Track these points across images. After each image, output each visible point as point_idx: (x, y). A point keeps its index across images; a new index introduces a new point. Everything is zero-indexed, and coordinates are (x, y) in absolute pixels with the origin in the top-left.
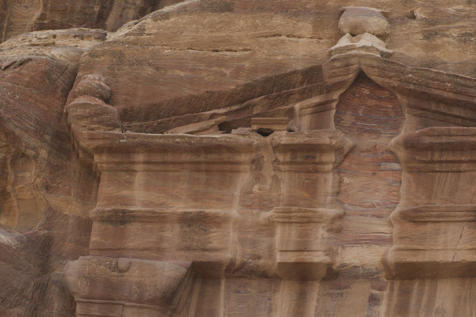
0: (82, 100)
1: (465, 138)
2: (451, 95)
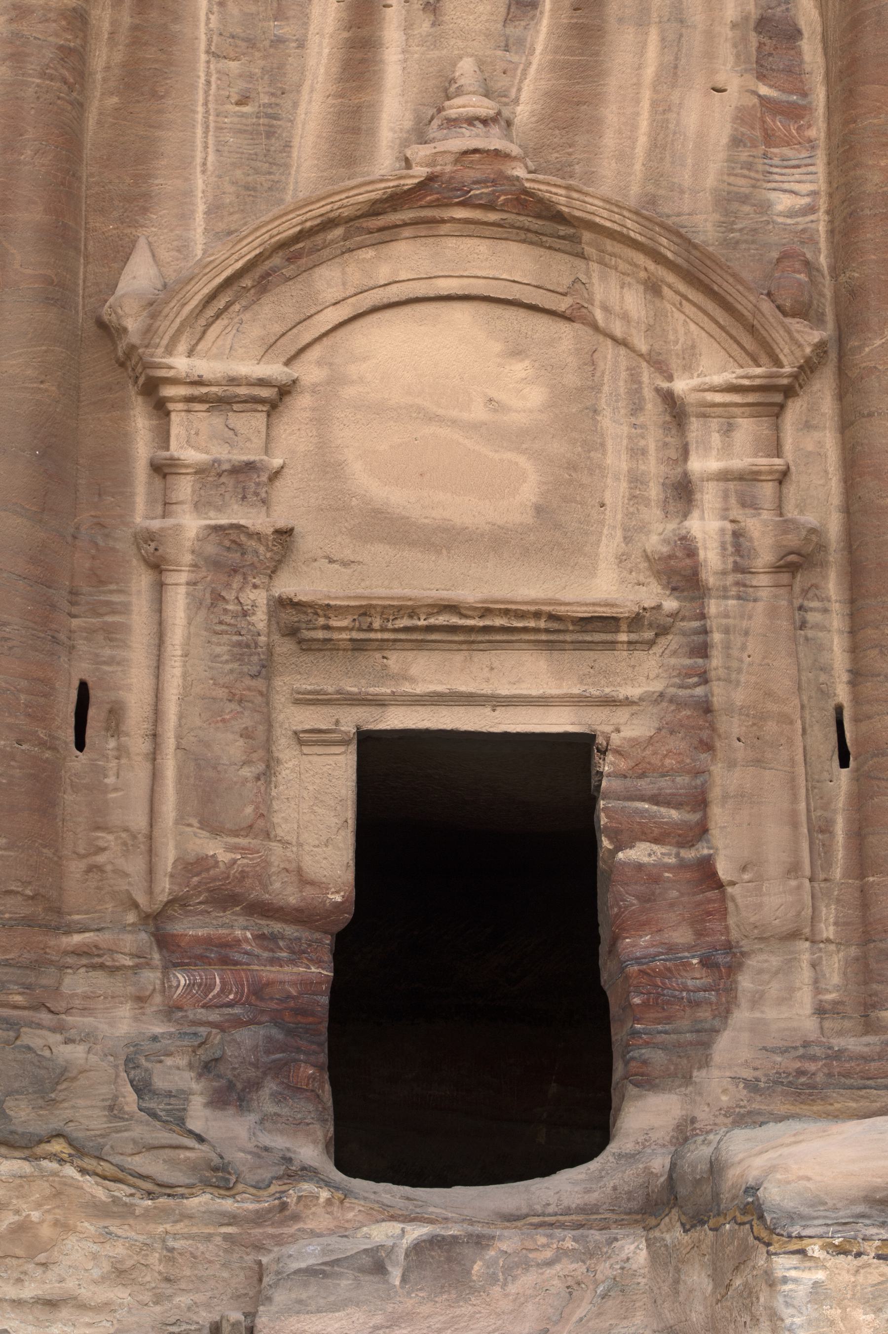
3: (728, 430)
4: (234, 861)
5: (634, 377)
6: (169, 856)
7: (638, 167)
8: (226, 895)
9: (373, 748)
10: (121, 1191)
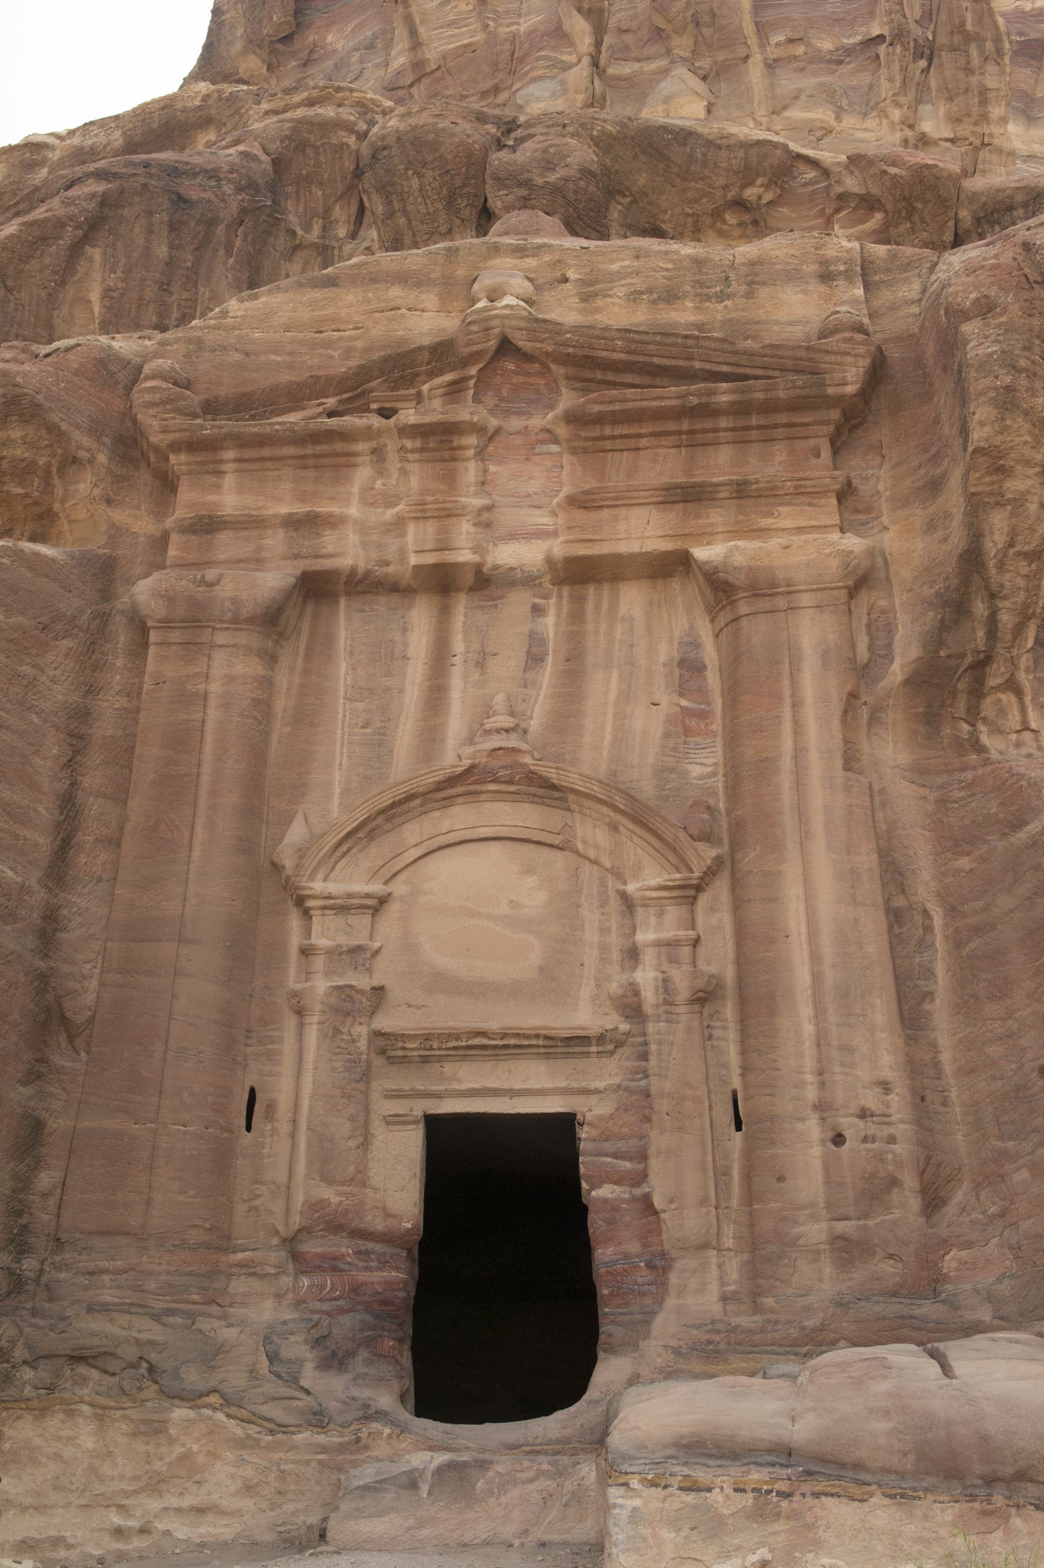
0: (150, 384)
1: (644, 403)
2: (623, 356)
3: (661, 914)
4: (341, 1202)
5: (603, 884)
6: (299, 1199)
7: (605, 754)
8: (337, 1225)
10: (252, 1430)
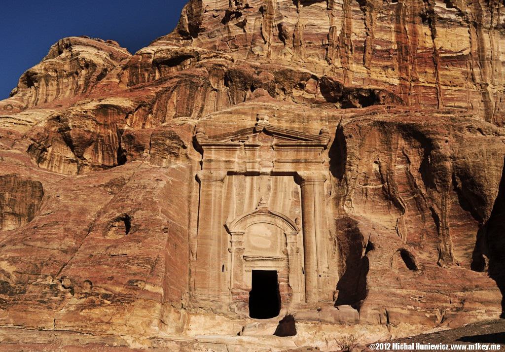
5: (281, 231)
9: (253, 272)
